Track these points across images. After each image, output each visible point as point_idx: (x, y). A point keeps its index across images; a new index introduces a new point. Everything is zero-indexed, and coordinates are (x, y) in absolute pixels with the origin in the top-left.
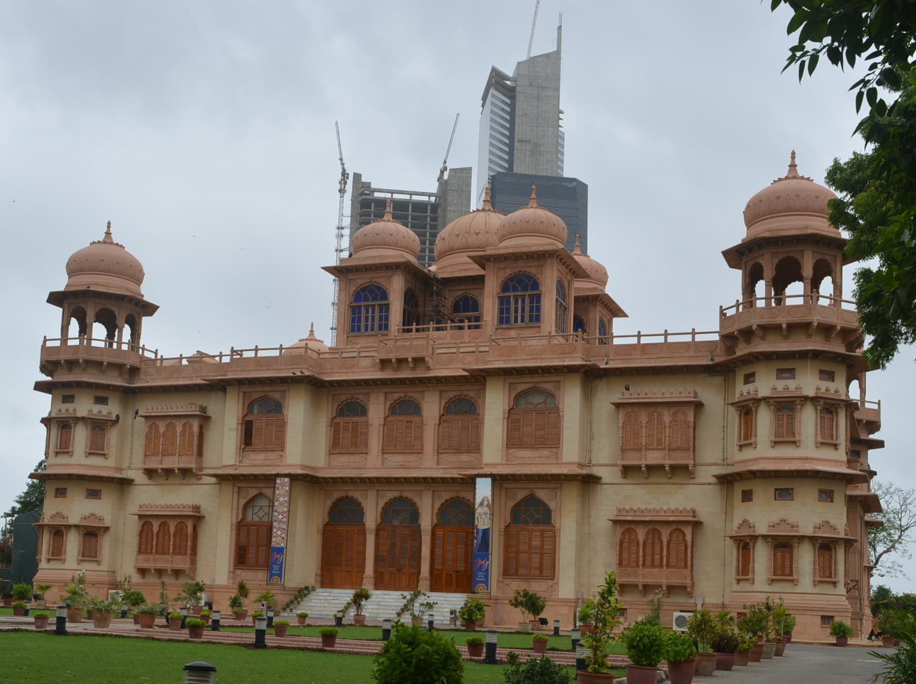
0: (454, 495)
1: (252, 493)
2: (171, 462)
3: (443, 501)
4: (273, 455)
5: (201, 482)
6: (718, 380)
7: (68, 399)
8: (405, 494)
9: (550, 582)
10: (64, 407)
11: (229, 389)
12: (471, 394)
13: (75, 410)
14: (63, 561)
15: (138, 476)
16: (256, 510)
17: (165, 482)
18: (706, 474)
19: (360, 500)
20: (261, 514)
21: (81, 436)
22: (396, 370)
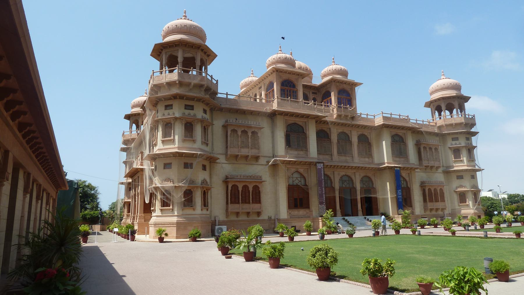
0: (365, 174)
1: (293, 170)
2: (244, 152)
3: (361, 177)
4: (301, 153)
5: (257, 163)
6: (438, 138)
7: (187, 107)
8: (348, 174)
9: (410, 208)
10: (187, 112)
11: (278, 116)
12: (366, 134)
13: (195, 115)
14: (194, 209)
15: (222, 159)
16: (294, 179)
17: (236, 162)
18: (440, 170)
19: (330, 176)
20: (297, 182)
21: (198, 131)
22: (341, 119)
